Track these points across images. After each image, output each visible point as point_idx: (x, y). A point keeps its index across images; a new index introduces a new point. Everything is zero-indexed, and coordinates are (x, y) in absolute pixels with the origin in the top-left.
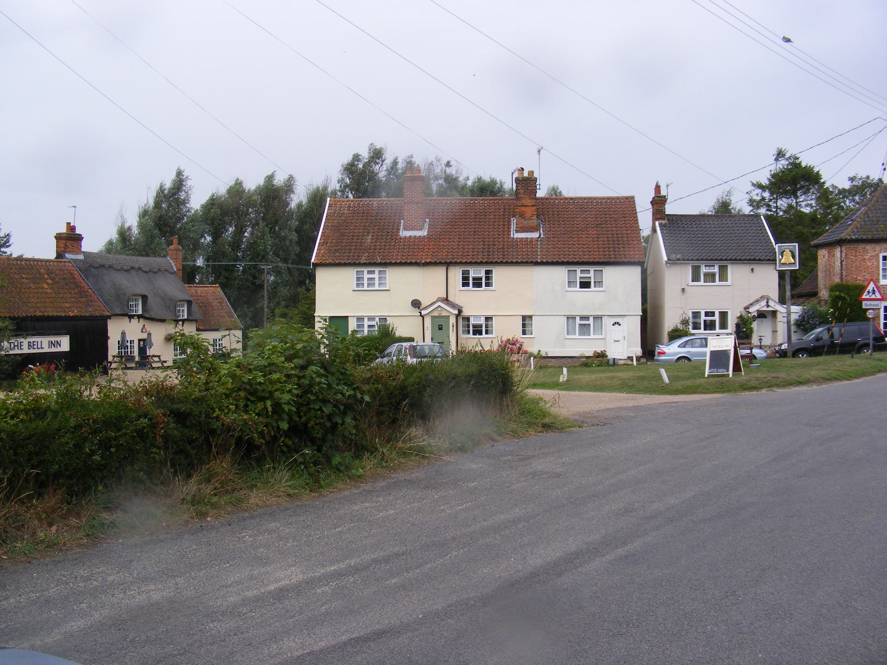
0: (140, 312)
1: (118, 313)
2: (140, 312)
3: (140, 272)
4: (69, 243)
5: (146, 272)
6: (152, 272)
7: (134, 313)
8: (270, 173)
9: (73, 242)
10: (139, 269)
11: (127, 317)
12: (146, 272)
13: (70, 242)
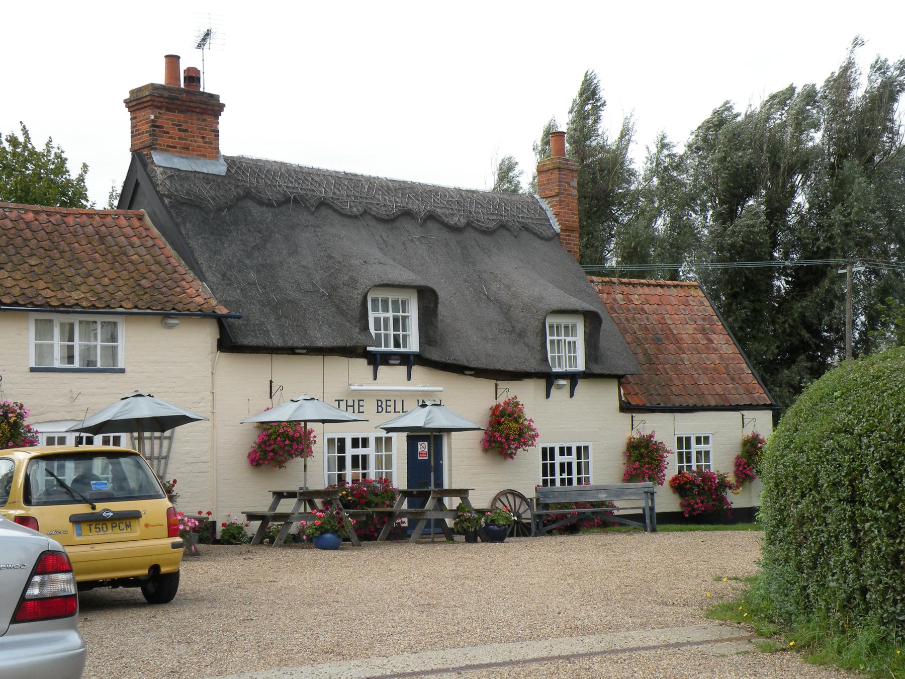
0: (413, 345)
1: (320, 344)
2: (413, 345)
3: (435, 232)
4: (168, 120)
5: (455, 229)
6: (475, 228)
7: (392, 348)
8: (835, 68)
9: (182, 117)
10: (432, 217)
11: (364, 361)
12: (455, 229)
13: (170, 115)
